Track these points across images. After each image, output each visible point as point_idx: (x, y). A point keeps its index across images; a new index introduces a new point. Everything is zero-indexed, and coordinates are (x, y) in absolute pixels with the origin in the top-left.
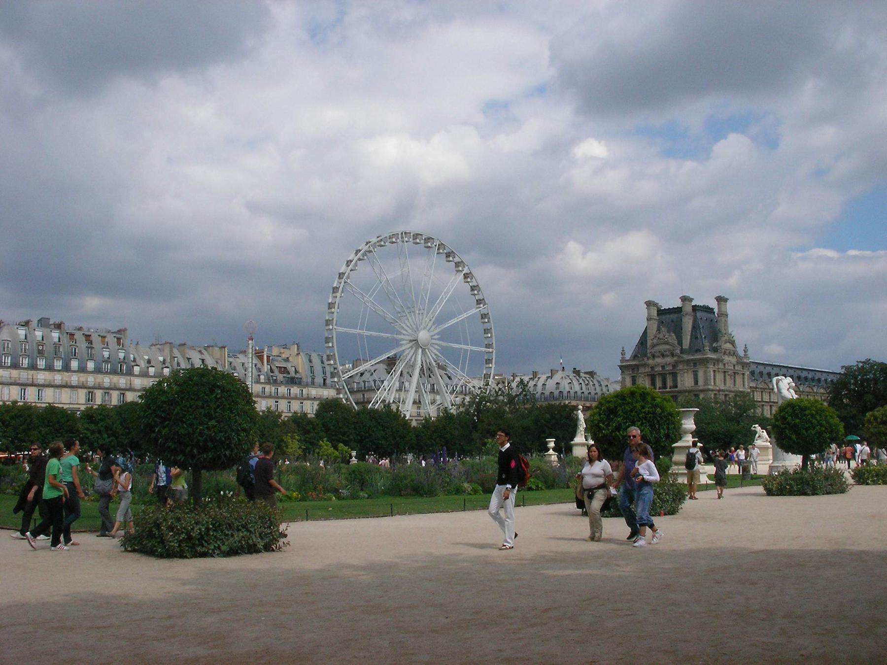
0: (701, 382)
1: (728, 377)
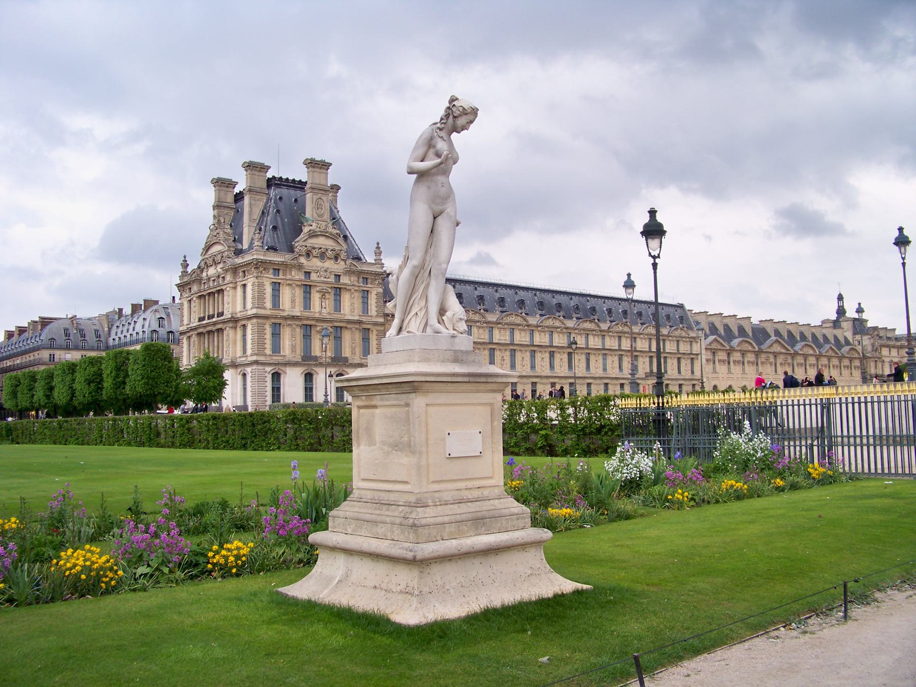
0: (249, 305)
1: (316, 297)
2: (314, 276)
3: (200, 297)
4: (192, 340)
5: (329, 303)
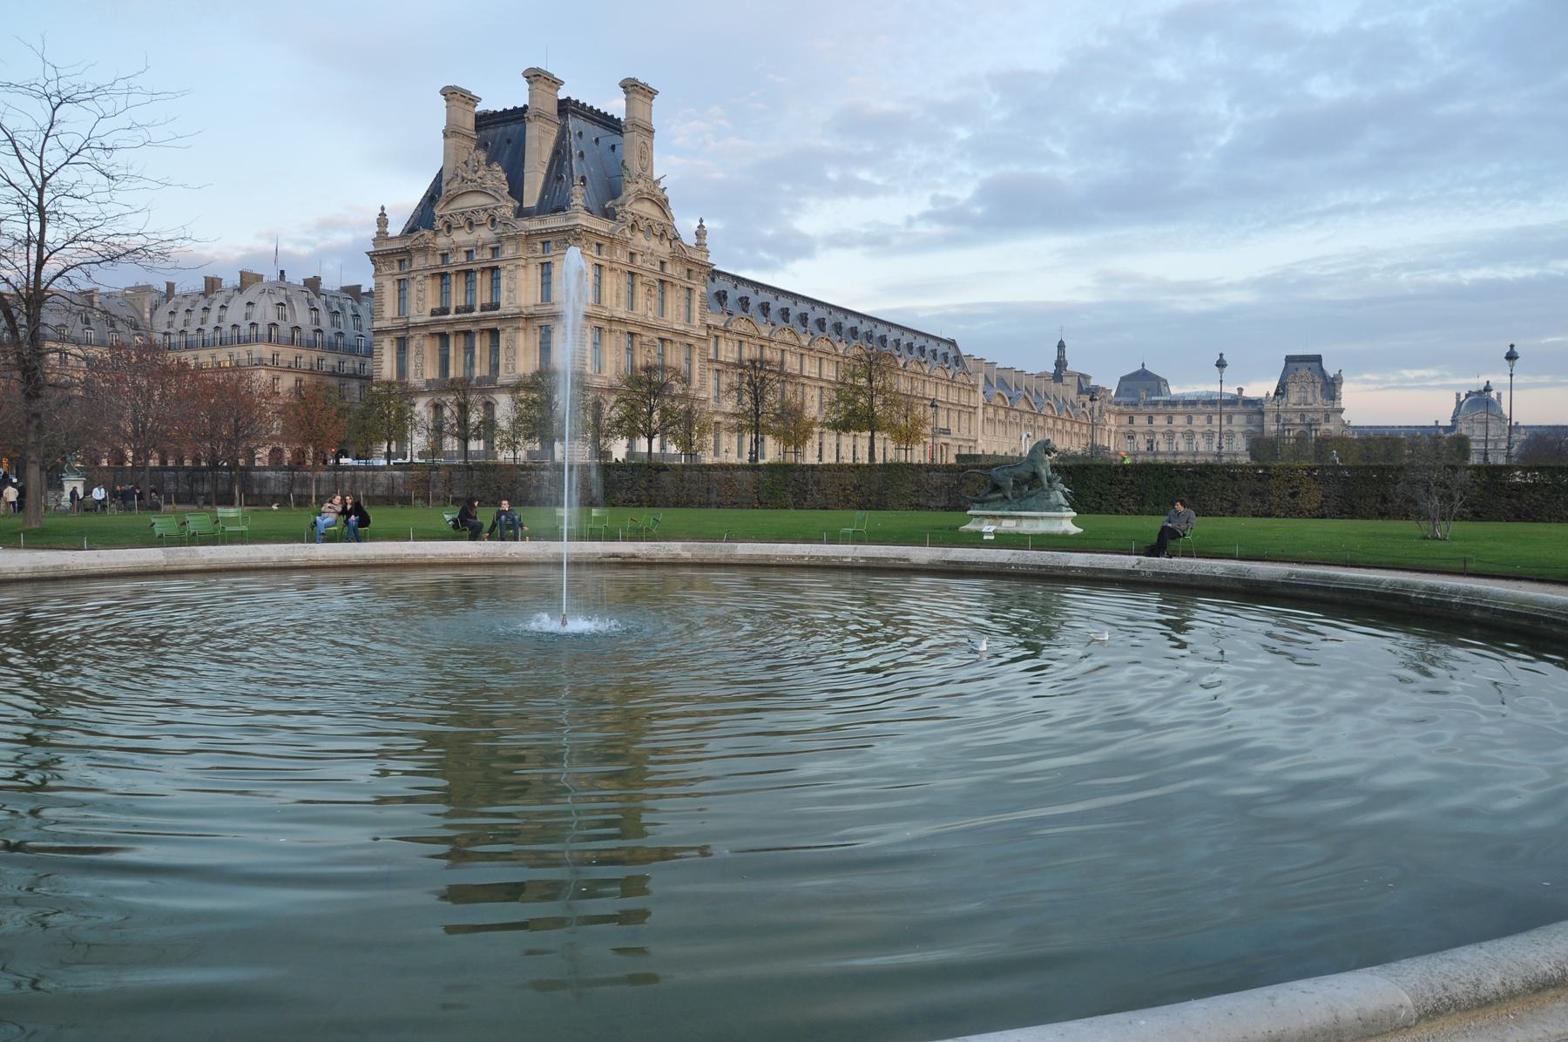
1: (640, 291)
2: (638, 259)
3: (434, 275)
4: (412, 347)
5: (654, 302)
